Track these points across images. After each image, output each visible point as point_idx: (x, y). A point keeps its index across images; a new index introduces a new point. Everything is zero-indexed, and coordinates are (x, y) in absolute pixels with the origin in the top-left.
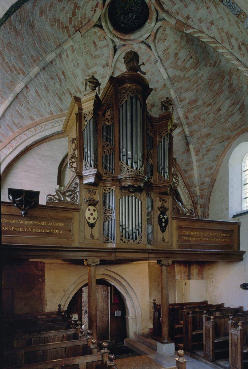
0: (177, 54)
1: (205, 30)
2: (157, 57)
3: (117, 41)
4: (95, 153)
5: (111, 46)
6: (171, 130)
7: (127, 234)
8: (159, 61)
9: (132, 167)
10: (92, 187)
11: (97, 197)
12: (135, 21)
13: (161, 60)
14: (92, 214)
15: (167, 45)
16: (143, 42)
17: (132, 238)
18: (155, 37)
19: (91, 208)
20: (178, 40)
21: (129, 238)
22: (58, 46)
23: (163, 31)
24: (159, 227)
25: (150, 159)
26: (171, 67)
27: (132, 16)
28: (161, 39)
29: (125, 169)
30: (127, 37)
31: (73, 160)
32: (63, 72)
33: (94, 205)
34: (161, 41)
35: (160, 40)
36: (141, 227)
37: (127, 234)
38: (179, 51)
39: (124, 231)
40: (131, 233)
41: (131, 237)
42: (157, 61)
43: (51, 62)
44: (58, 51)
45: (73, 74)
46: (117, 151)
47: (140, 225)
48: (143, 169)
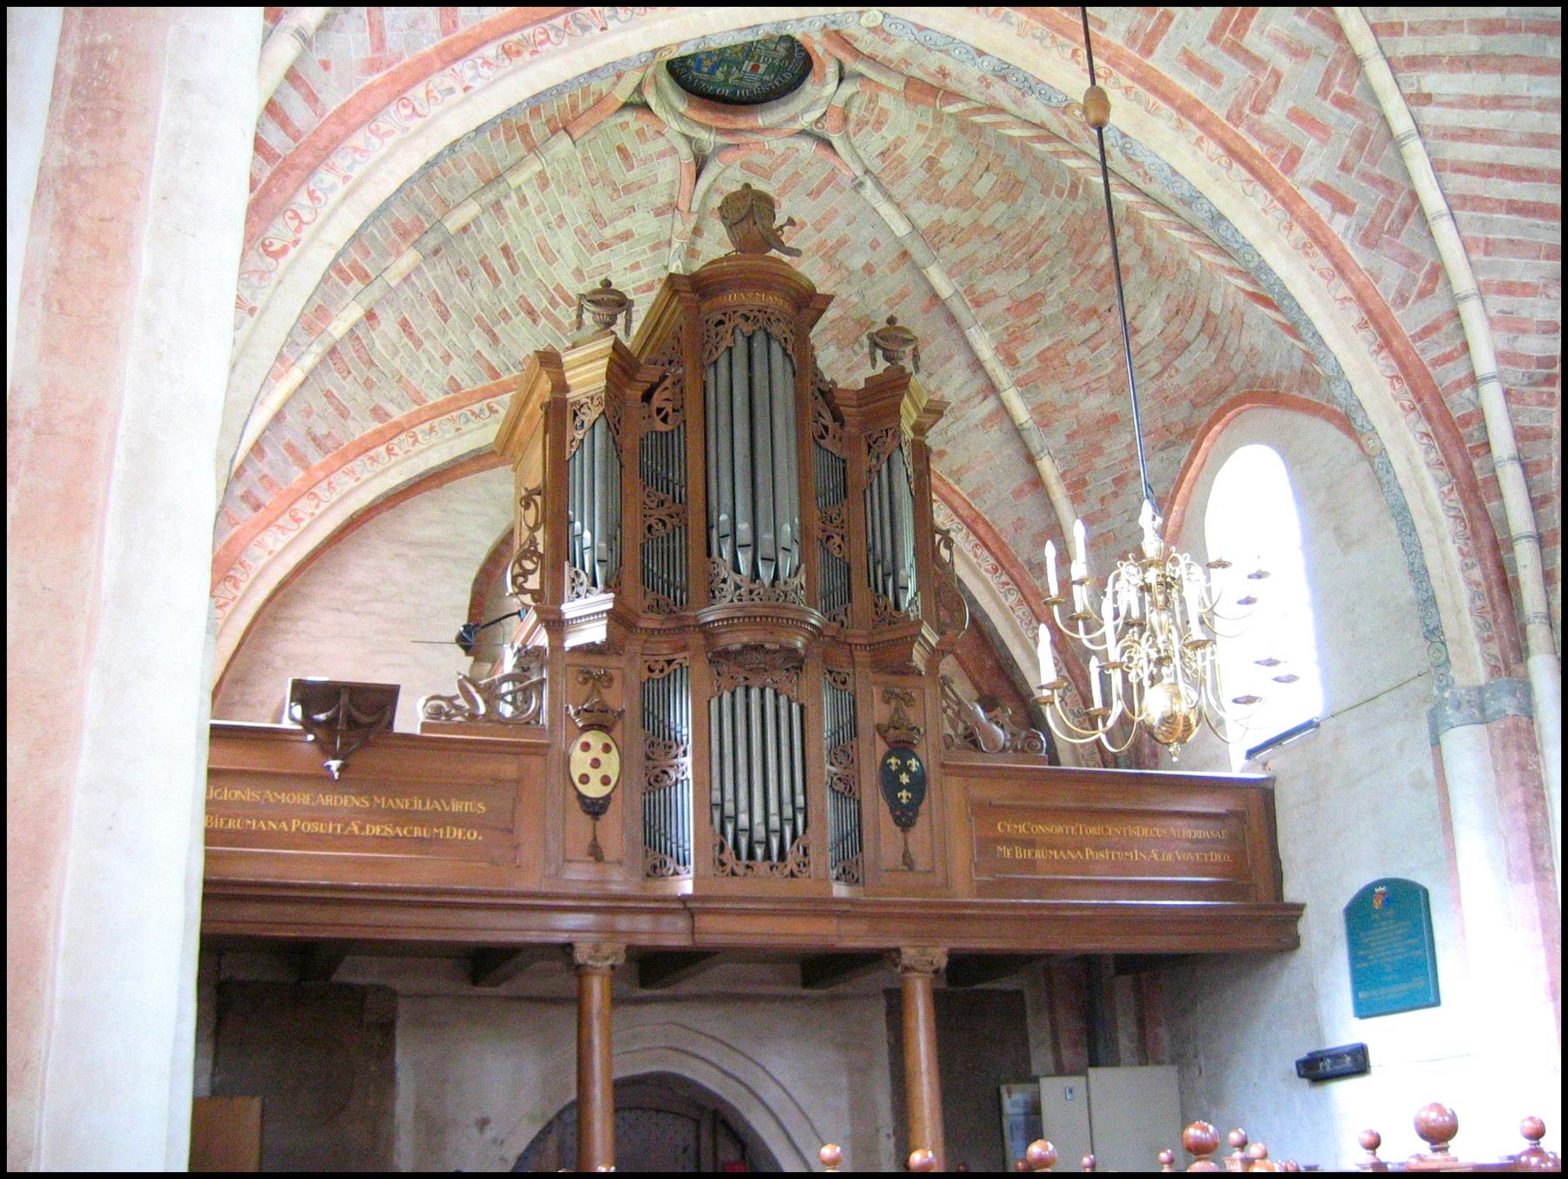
0: (931, 162)
1: (1009, 105)
2: (859, 173)
3: (707, 139)
4: (614, 536)
5: (685, 151)
6: (919, 429)
7: (744, 841)
8: (869, 183)
9: (755, 574)
10: (598, 660)
11: (614, 698)
12: (766, 78)
13: (877, 182)
14: (596, 763)
15: (891, 138)
16: (803, 133)
17: (767, 856)
18: (846, 119)
19: (595, 739)
20: (930, 125)
21: (751, 855)
22: (489, 183)
23: (870, 101)
24: (884, 809)
25: (837, 540)
26: (919, 198)
27: (755, 68)
28: (867, 123)
29: (729, 587)
30: (742, 122)
31: (529, 565)
32: (506, 251)
33: (604, 728)
34: (869, 128)
35: (862, 124)
36: (805, 810)
37: (744, 841)
38: (938, 151)
39: (730, 828)
40: (759, 832)
41: (759, 851)
42: (861, 184)
43: (465, 229)
44: (490, 196)
45: (543, 249)
46: (695, 521)
47: (800, 800)
48: (802, 578)
